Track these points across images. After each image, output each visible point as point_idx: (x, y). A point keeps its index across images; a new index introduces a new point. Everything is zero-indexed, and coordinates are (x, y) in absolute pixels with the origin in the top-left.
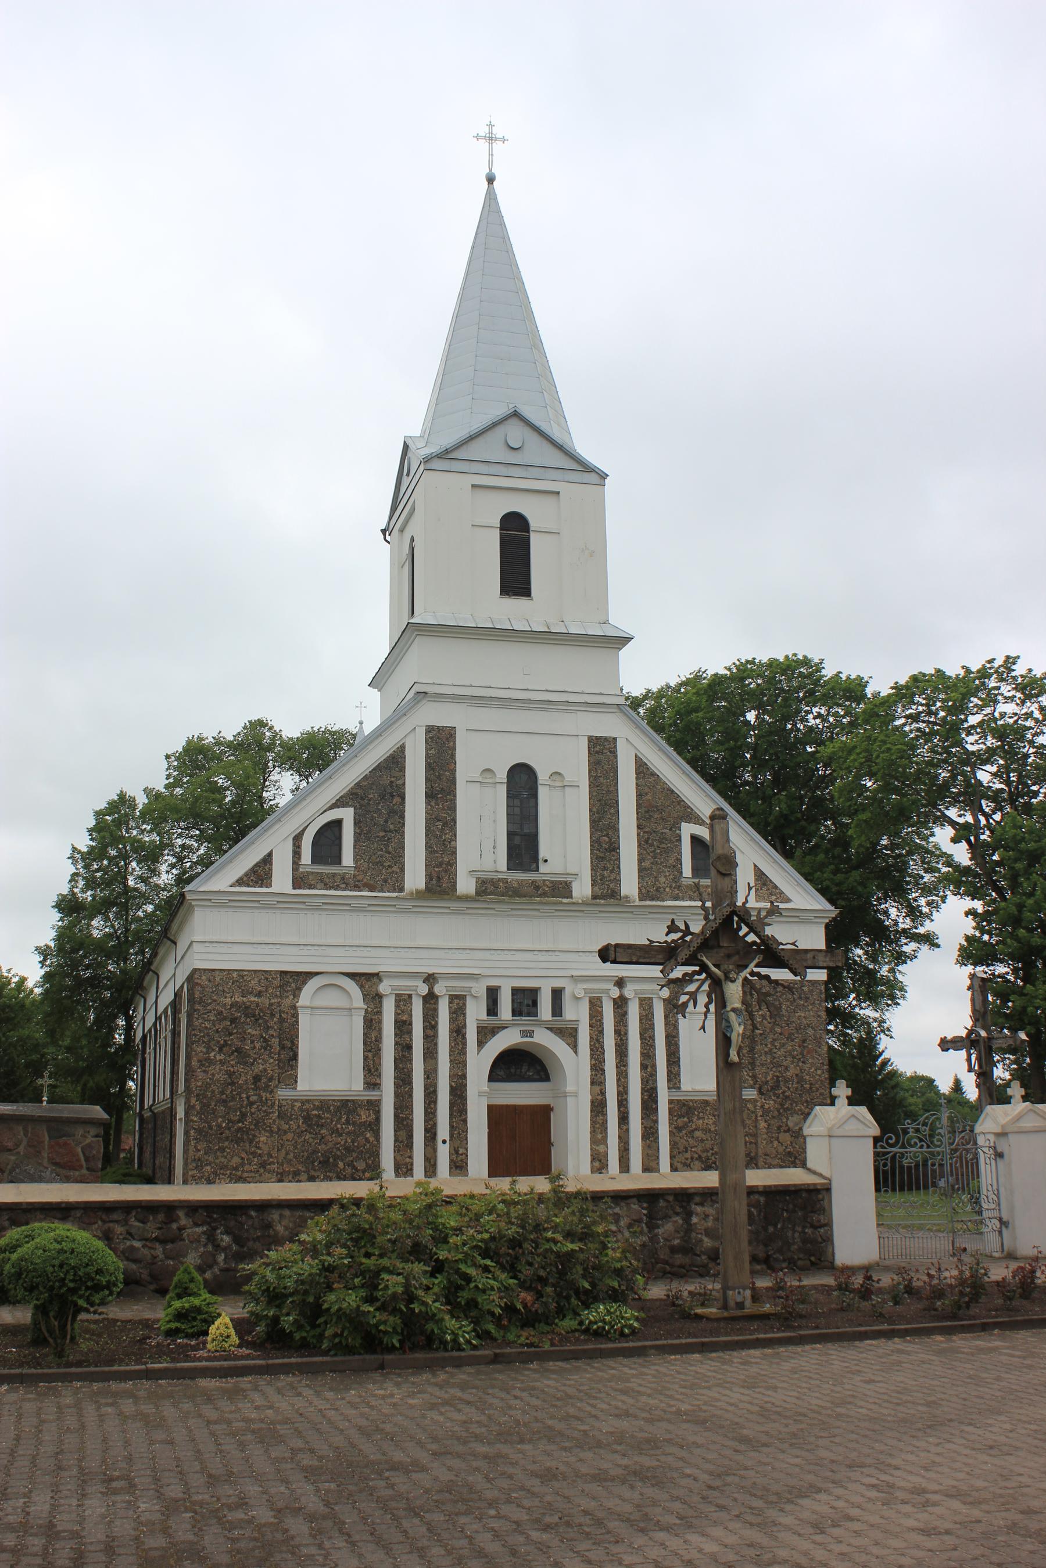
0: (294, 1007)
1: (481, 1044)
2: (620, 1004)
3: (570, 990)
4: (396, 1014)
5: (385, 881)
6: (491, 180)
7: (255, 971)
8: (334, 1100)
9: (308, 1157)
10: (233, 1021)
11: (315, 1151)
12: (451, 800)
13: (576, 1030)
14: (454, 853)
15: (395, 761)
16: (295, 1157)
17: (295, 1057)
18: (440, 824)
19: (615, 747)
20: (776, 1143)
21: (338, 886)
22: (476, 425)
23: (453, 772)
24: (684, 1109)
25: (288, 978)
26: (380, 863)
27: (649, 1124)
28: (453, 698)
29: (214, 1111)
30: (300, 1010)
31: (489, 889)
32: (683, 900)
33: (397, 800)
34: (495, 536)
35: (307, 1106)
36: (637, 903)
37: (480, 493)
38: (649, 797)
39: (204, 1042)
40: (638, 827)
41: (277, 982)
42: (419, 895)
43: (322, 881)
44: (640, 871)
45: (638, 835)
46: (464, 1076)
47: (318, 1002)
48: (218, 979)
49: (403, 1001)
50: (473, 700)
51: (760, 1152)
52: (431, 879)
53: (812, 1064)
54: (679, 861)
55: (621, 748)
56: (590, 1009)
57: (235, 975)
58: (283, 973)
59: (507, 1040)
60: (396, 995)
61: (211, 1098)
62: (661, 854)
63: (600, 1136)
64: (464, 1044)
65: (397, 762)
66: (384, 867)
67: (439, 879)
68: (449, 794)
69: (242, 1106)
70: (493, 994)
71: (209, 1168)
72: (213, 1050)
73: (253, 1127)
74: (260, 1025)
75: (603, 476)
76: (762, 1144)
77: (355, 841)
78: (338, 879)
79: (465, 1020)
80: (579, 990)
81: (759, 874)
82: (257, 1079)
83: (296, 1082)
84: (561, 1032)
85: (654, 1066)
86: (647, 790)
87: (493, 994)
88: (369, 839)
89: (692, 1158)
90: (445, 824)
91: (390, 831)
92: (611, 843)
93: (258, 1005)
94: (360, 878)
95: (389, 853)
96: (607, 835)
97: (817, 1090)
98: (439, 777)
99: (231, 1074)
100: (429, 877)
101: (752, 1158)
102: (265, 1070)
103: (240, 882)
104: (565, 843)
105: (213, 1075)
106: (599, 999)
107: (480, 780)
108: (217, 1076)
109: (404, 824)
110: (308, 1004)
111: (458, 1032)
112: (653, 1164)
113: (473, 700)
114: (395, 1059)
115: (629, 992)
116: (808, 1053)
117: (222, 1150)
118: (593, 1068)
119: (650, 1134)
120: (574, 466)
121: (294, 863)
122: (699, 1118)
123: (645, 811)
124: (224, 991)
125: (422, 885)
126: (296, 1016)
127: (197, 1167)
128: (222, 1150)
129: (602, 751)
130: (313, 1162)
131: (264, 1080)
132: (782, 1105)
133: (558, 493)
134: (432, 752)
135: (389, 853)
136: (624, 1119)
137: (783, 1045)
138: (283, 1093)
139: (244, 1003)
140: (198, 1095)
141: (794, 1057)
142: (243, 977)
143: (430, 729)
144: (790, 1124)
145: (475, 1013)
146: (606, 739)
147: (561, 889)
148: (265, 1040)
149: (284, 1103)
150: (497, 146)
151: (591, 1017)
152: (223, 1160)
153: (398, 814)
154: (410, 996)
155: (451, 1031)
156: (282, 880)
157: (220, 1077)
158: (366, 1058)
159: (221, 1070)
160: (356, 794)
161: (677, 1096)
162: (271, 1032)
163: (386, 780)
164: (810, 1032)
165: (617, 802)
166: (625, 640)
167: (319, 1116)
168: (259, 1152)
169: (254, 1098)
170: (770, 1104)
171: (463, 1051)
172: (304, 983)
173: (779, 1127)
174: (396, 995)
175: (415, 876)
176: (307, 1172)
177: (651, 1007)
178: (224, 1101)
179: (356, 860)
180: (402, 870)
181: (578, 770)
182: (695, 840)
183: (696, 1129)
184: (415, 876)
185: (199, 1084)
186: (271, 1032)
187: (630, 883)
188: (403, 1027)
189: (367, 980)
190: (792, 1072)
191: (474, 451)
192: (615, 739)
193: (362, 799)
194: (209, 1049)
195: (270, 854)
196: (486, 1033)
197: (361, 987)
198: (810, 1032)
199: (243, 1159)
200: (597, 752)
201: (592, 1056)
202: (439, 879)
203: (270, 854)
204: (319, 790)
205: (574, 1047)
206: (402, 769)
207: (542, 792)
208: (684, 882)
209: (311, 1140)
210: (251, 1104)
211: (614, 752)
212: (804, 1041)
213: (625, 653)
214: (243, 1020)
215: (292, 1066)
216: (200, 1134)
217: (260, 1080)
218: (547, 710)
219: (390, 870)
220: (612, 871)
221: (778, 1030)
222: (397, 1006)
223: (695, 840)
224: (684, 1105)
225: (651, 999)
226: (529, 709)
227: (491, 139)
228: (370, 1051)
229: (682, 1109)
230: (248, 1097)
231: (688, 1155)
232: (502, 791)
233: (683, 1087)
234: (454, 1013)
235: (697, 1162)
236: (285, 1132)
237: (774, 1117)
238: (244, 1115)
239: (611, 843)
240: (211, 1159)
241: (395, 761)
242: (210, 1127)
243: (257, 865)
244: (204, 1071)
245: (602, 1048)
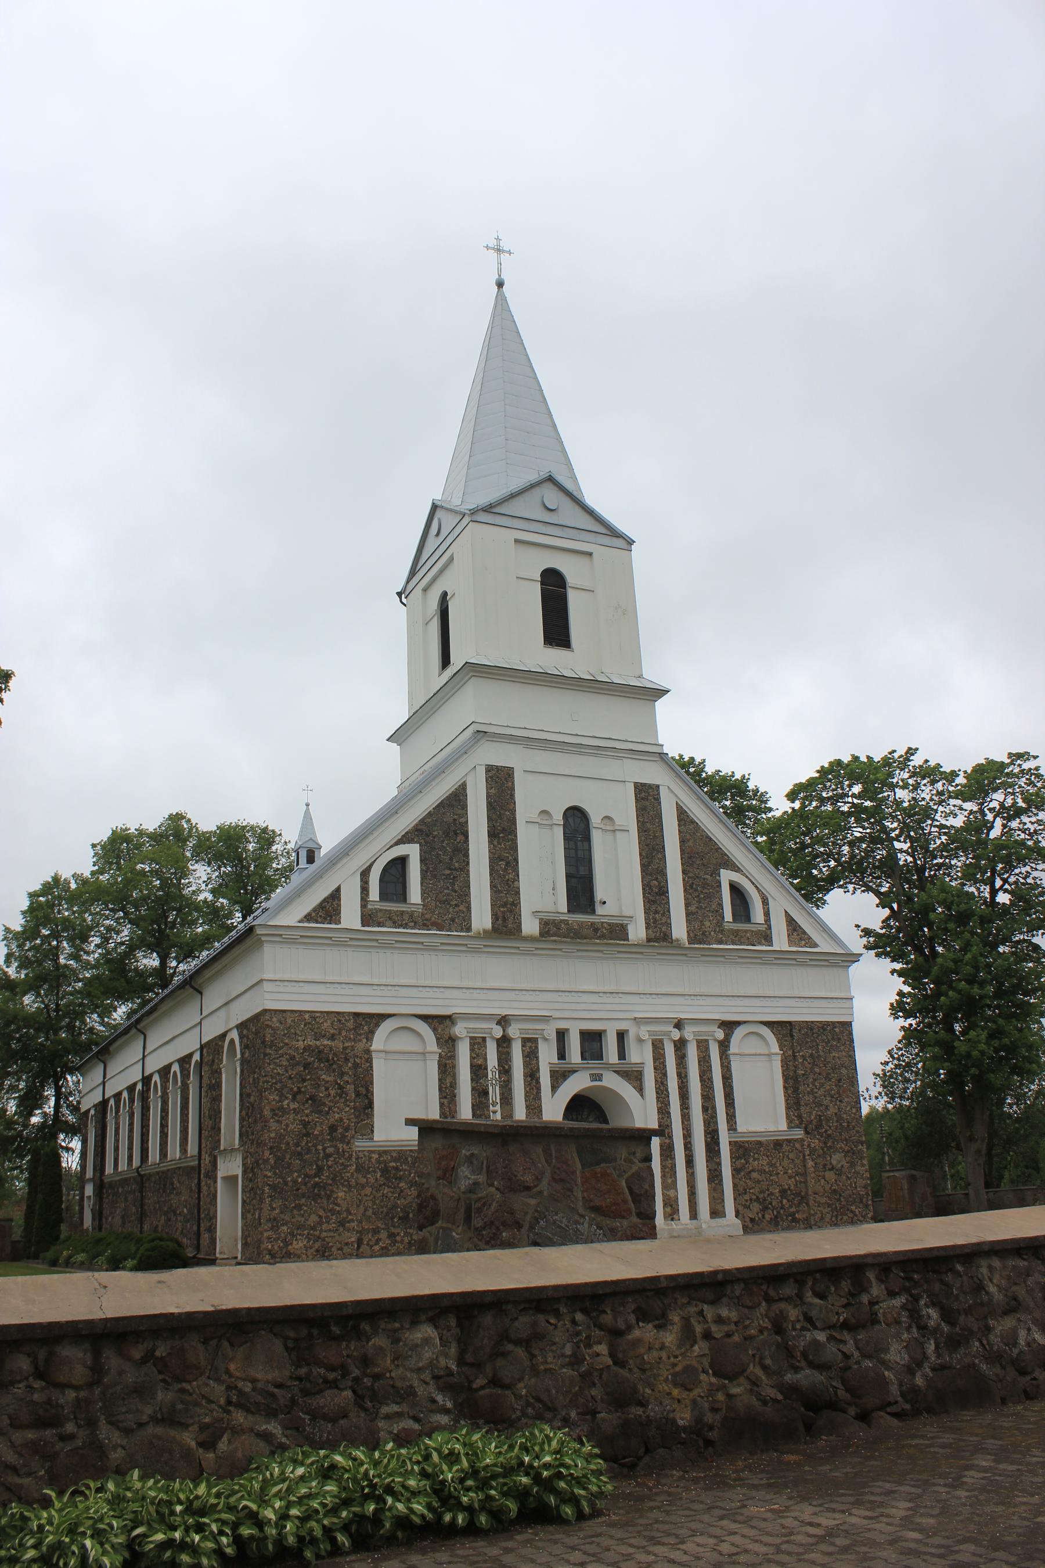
0: (368, 1052)
1: (554, 1088)
2: (680, 1045)
4: (472, 1058)
5: (453, 920)
6: (500, 284)
7: (328, 1013)
8: (411, 1151)
9: (387, 1214)
10: (306, 1066)
11: (395, 1206)
12: (512, 840)
14: (518, 893)
15: (457, 799)
16: (374, 1213)
17: (370, 1105)
18: (503, 864)
19: (659, 794)
20: (823, 1181)
21: (406, 924)
22: (515, 485)
23: (513, 812)
24: (741, 1151)
25: (360, 1020)
26: (447, 902)
27: (713, 1166)
28: (511, 739)
29: (289, 1165)
30: (374, 1055)
31: (551, 929)
32: (726, 944)
33: (461, 838)
34: (537, 589)
35: (384, 1158)
36: (687, 945)
37: (523, 550)
38: (690, 843)
39: (276, 1089)
40: (684, 872)
41: (351, 1024)
42: (486, 934)
43: (390, 919)
44: (687, 915)
45: (684, 880)
47: (392, 1047)
48: (289, 1021)
49: (477, 1044)
50: (528, 742)
51: (810, 1192)
52: (497, 920)
53: (847, 1102)
54: (721, 905)
55: (663, 793)
57: (307, 1016)
58: (356, 1015)
59: (577, 1084)
60: (471, 1038)
61: (285, 1151)
62: (704, 899)
63: (670, 1181)
64: (539, 1089)
65: (460, 800)
66: (451, 905)
67: (504, 919)
68: (510, 833)
69: (318, 1159)
70: (562, 1035)
71: (285, 1228)
72: (287, 1098)
73: (330, 1182)
74: (334, 1071)
75: (631, 542)
76: (811, 1182)
77: (422, 879)
78: (406, 917)
80: (644, 1032)
81: (791, 922)
82: (333, 1128)
83: (373, 1131)
85: (714, 1108)
86: (688, 836)
87: (562, 1035)
88: (434, 876)
89: (751, 1200)
90: (508, 864)
91: (455, 869)
92: (660, 887)
93: (331, 1049)
94: (428, 916)
95: (456, 892)
96: (656, 879)
97: (854, 1128)
98: (500, 816)
99: (305, 1124)
100: (495, 917)
101: (802, 1198)
102: (341, 1119)
103: (308, 918)
104: (619, 889)
105: (287, 1125)
106: (661, 1041)
107: (538, 820)
108: (291, 1127)
109: (468, 863)
110: (381, 1047)
111: (532, 1076)
112: (719, 1207)
113: (528, 742)
114: (473, 1105)
115: (689, 1033)
116: (844, 1092)
117: (299, 1207)
119: (715, 1176)
120: (604, 531)
121: (362, 899)
122: (755, 1160)
123: (688, 858)
124: (296, 1034)
125: (488, 924)
126: (370, 1061)
127: (272, 1228)
128: (299, 1207)
129: (647, 797)
130: (392, 1218)
131: (340, 1130)
132: (825, 1143)
133: (590, 554)
134: (492, 791)
135: (456, 892)
136: (690, 1162)
137: (822, 1085)
138: (360, 1144)
139: (317, 1047)
140: (271, 1148)
141: (832, 1097)
142: (315, 1018)
143: (489, 769)
144: (834, 1162)
145: (547, 1056)
146: (650, 786)
147: (617, 931)
148: (341, 1087)
149: (361, 1155)
150: (504, 257)
151: (655, 1059)
152: (300, 1219)
153: (462, 851)
154: (484, 1039)
155: (525, 1076)
156: (350, 916)
157: (295, 1127)
158: (442, 1105)
159: (295, 1120)
160: (421, 830)
162: (346, 1078)
163: (449, 818)
164: (844, 1071)
165: (663, 847)
166: (663, 692)
167: (397, 1169)
168: (338, 1208)
169: (330, 1150)
170: (816, 1143)
171: (538, 1097)
172: (377, 1025)
173: (825, 1166)
174: (471, 1038)
175: (482, 916)
176: (387, 1229)
177: (707, 1049)
178: (300, 1154)
179: (423, 899)
180: (469, 909)
181: (627, 815)
182: (735, 888)
183: (753, 1171)
184: (482, 916)
185: (273, 1135)
186: (346, 1078)
187: (679, 929)
188: (478, 1070)
189: (439, 1022)
190: (832, 1110)
191: (515, 508)
192: (658, 786)
193: (427, 835)
194: (282, 1097)
195: (338, 890)
196: (559, 1077)
197: (434, 1030)
198: (844, 1071)
199: (320, 1217)
200: (643, 799)
202: (504, 919)
203: (338, 890)
204: (386, 825)
205: (640, 1090)
206: (465, 807)
207: (596, 836)
208: (727, 926)
209: (390, 1194)
210: (327, 1156)
211: (658, 799)
212: (839, 1081)
213: (660, 704)
214: (316, 1065)
215: (367, 1115)
216: (275, 1191)
217: (336, 1130)
218: (595, 755)
219: (457, 909)
220: (663, 915)
221: (817, 1070)
222: (472, 1050)
223: (735, 888)
224: (741, 1146)
225: (707, 1041)
226: (580, 753)
227: (499, 250)
228: (445, 1097)
229: (742, 1150)
230: (324, 1149)
231: (747, 1197)
232: (559, 833)
233: (739, 1129)
234: (527, 1056)
235: (755, 1204)
236: (363, 1187)
237: (819, 1156)
238: (320, 1169)
239: (660, 887)
240: (287, 1218)
241: (457, 799)
242: (286, 1183)
243: (325, 900)
244: (278, 1121)
245: (667, 1090)
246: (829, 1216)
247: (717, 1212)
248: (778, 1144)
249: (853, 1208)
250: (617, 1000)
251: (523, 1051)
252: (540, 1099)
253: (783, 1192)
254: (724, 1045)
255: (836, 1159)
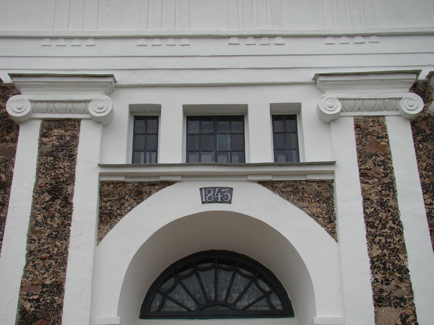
1: (108, 217)
3: (311, 105)
13: (329, 185)
46: (58, 288)
56: (359, 142)
64: (67, 216)
70: (145, 122)
79: (72, 168)
84: (295, 192)
87: (145, 122)
106: (379, 121)
111: (55, 193)
118: (377, 264)
145: (99, 153)
151: (362, 157)
155: (39, 190)
171: (62, 233)
201: (371, 238)
205: (328, 220)
245: (396, 219)
250: (272, 49)
251: (42, 144)
252: (66, 237)
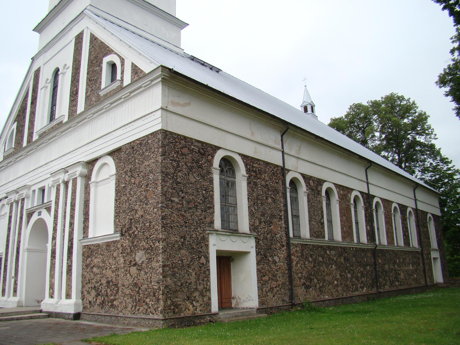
27: (69, 264)
97: (154, 226)
161: (86, 242)
183: (94, 266)
229: (89, 252)
246: (130, 306)
247: (68, 296)
248: (108, 245)
249: (148, 300)
253: (108, 282)
254: (88, 177)
255: (140, 256)
